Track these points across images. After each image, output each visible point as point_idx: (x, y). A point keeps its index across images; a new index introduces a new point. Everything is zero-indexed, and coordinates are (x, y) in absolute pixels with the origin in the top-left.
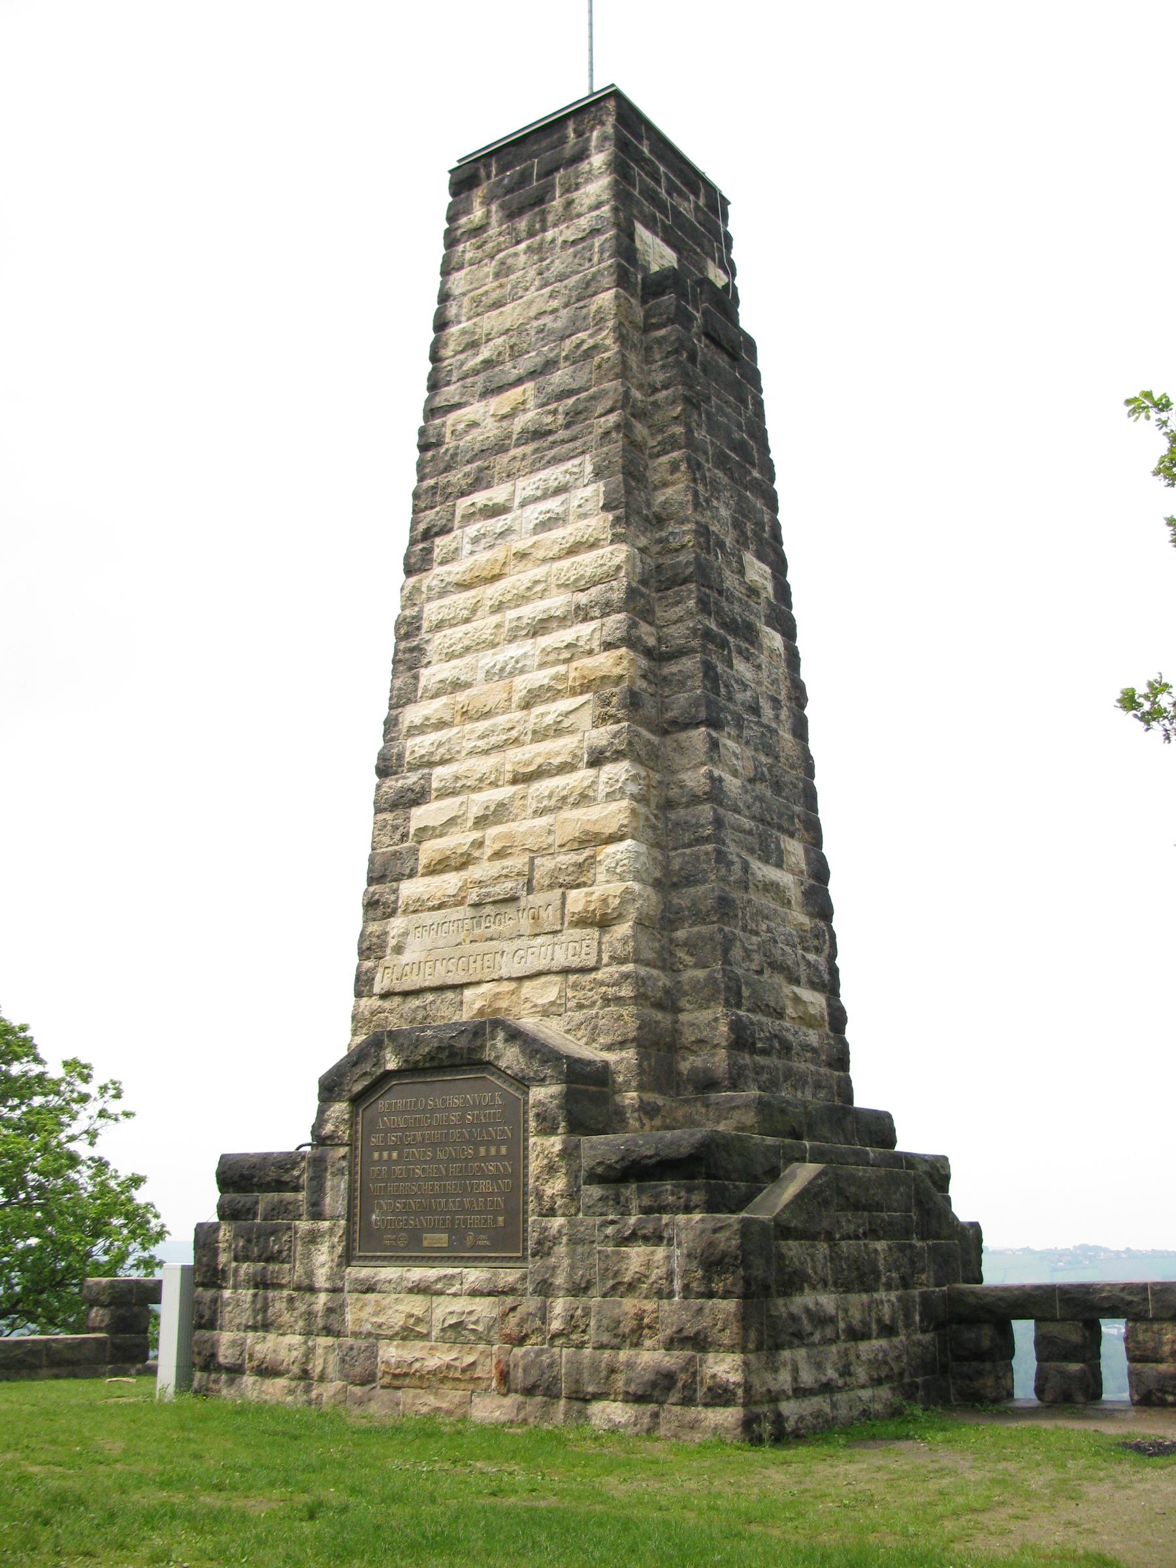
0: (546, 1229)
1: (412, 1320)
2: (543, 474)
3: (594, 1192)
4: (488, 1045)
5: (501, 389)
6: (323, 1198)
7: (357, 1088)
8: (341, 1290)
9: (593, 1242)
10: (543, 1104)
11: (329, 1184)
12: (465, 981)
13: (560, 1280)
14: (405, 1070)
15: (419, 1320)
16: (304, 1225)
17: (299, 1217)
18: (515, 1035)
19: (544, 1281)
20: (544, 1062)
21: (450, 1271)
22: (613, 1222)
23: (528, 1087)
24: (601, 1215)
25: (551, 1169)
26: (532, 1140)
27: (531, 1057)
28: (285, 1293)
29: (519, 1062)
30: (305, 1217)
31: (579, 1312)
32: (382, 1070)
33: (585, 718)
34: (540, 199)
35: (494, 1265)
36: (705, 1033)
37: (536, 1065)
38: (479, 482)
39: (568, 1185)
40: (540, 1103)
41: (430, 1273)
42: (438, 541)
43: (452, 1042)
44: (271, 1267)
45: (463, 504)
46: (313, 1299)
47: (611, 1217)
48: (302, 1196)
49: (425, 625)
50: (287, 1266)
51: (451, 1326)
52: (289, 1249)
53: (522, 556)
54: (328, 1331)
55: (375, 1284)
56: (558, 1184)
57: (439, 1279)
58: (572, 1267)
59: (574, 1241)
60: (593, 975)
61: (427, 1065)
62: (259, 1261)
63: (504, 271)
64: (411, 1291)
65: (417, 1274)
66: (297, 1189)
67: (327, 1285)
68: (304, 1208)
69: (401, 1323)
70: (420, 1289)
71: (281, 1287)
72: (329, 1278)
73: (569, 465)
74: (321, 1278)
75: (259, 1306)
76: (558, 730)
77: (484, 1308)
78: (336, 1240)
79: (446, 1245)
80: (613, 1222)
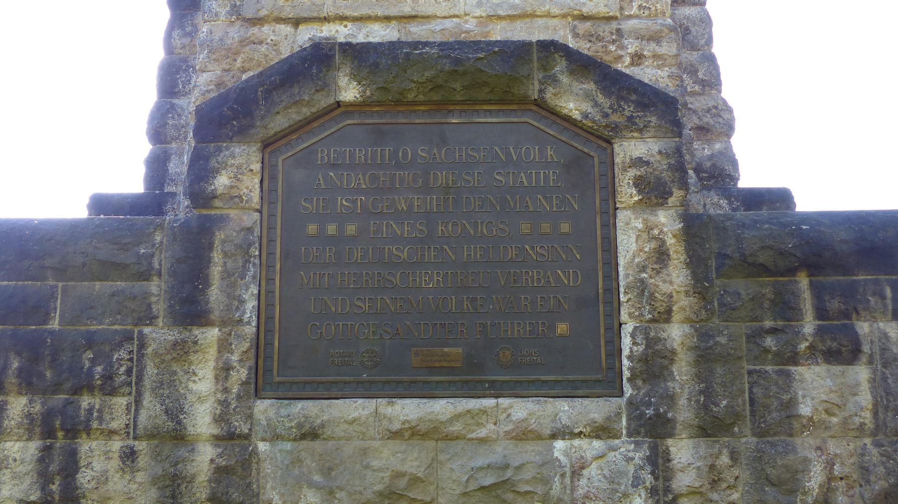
0: (658, 340)
1: (402, 483)
3: (743, 287)
4: (538, 75)
6: (204, 291)
7: (279, 122)
8: (247, 437)
9: (740, 358)
10: (648, 163)
11: (216, 271)
13: (684, 413)
14: (379, 103)
15: (415, 480)
17: (151, 319)
18: (583, 65)
19: (658, 415)
20: (643, 106)
21: (473, 404)
22: (773, 331)
23: (609, 142)
24: (755, 319)
25: (661, 256)
27: (620, 98)
29: (596, 104)
30: (160, 322)
31: (725, 459)
32: (331, 101)
35: (552, 392)
36: (706, 120)
37: (629, 110)
39: (694, 275)
41: (441, 408)
43: (479, 65)
44: (86, 401)
46: (183, 452)
47: (768, 324)
48: (155, 287)
50: (121, 402)
51: (483, 488)
52: (129, 372)
55: (322, 426)
56: (676, 278)
57: (457, 417)
58: (707, 393)
59: (705, 356)
60: (614, 25)
61: (421, 97)
62: (54, 392)
64: (396, 435)
65: (408, 410)
66: (145, 276)
67: (216, 431)
68: (160, 307)
69: (378, 487)
70: (413, 433)
72: (220, 419)
75: (54, 467)
78: (235, 358)
79: (458, 365)
80: (773, 331)
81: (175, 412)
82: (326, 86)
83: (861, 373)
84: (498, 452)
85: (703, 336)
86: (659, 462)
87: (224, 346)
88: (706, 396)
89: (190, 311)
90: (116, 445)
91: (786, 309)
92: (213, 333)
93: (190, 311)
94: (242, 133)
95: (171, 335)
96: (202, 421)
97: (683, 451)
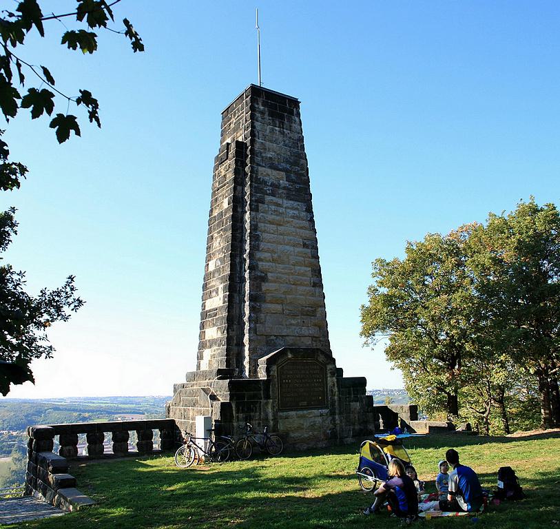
2: (292, 202)
5: (276, 169)
12: (286, 334)
13: (337, 411)
16: (263, 401)
26: (329, 378)
28: (257, 422)
33: (309, 274)
34: (282, 118)
38: (273, 195)
40: (331, 369)
42: (260, 205)
45: (268, 198)
49: (260, 229)
53: (288, 222)
54: (274, 431)
56: (336, 389)
63: (272, 131)
71: (256, 420)
73: (299, 203)
74: (270, 416)
76: (303, 275)
77: (319, 419)
81: (267, 415)
82: (287, 355)
83: (358, 404)
84: (312, 419)
85: (340, 398)
86: (334, 419)
87: (273, 403)
88: (340, 410)
89: (267, 397)
90: (257, 422)
91: (350, 394)
92: (271, 400)
93: (267, 397)
94: (274, 364)
95: (265, 401)
96: (270, 416)
97: (337, 417)
